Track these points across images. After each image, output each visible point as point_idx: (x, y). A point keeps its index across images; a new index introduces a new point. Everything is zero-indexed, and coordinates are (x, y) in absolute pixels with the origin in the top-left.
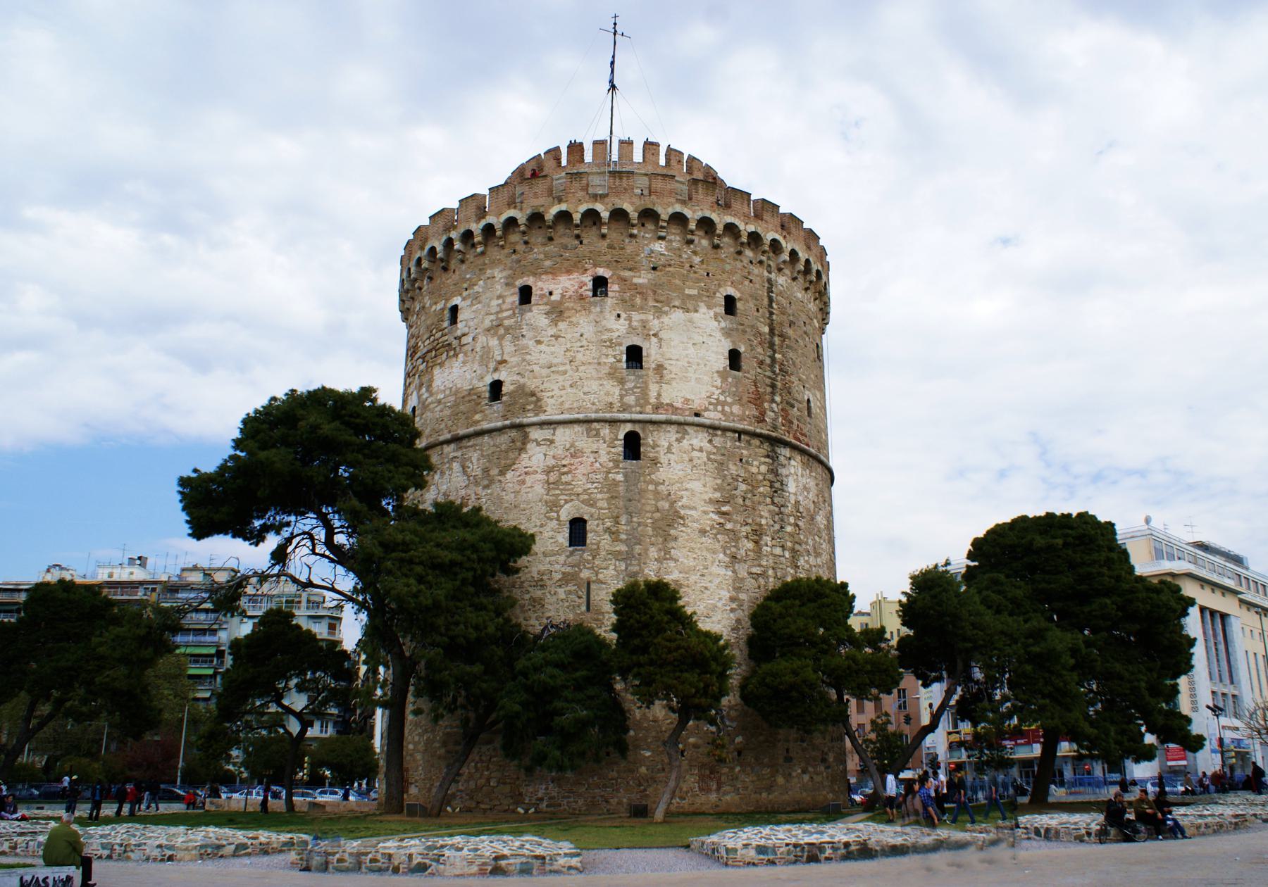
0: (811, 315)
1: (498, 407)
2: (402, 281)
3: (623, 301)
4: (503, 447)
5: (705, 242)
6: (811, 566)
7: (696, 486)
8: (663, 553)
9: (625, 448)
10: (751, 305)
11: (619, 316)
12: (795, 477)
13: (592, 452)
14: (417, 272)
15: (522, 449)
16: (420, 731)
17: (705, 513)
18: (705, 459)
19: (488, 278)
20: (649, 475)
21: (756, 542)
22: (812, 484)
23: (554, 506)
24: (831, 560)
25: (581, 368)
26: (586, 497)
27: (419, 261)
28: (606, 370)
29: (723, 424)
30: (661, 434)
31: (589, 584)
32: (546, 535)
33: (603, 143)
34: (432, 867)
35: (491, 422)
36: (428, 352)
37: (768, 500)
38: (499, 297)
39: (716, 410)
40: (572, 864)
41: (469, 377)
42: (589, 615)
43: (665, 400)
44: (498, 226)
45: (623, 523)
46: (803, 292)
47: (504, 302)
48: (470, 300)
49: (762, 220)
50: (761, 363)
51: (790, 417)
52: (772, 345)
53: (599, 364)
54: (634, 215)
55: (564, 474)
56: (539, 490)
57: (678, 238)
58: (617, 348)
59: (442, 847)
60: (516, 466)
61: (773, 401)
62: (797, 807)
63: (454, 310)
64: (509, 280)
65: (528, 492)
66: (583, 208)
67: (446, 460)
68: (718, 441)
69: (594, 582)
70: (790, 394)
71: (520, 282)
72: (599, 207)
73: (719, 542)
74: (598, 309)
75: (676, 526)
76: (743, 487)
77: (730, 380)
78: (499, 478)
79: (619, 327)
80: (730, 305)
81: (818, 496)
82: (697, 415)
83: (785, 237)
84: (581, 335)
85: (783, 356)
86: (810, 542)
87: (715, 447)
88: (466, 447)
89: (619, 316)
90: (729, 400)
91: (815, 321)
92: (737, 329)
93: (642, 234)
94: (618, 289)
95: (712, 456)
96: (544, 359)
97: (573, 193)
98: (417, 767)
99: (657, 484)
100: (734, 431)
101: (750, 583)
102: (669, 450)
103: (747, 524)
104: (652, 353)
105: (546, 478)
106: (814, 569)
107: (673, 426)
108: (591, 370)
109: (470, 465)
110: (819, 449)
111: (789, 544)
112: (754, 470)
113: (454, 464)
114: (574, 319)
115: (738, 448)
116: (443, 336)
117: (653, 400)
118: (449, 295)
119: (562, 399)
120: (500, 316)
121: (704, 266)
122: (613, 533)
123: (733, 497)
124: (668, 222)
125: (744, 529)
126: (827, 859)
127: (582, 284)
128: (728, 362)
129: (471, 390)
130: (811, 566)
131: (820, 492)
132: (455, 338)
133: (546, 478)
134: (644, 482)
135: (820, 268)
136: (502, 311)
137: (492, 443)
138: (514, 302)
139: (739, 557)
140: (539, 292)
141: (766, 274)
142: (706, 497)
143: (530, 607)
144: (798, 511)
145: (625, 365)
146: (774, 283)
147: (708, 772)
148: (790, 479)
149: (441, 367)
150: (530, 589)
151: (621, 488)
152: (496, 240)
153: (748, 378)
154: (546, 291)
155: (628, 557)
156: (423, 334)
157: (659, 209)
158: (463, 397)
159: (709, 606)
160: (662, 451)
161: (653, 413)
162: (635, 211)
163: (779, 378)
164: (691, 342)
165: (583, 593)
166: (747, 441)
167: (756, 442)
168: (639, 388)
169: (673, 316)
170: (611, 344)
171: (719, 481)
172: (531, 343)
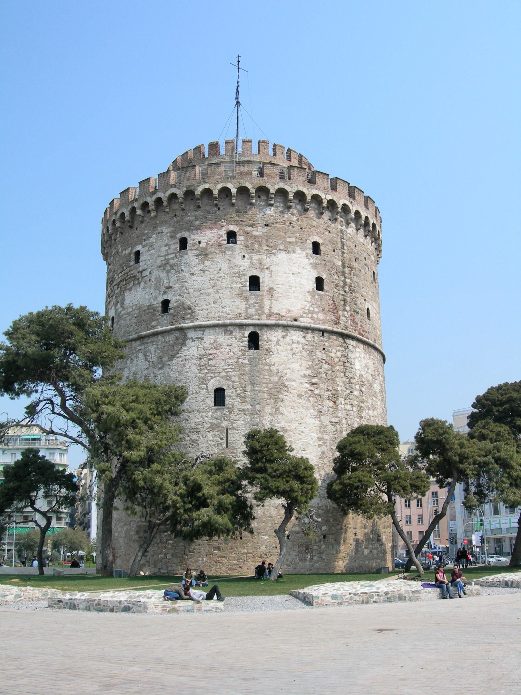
0: (370, 253)
1: (166, 317)
2: (103, 235)
3: (247, 246)
4: (171, 343)
5: (299, 207)
6: (370, 417)
7: (295, 366)
8: (274, 410)
9: (250, 341)
10: (330, 248)
11: (244, 256)
12: (360, 359)
13: (228, 345)
14: (113, 229)
15: (183, 344)
16: (122, 524)
17: (301, 383)
18: (301, 349)
19: (159, 233)
20: (265, 359)
21: (335, 402)
22: (370, 363)
23: (204, 381)
24: (383, 412)
25: (220, 291)
26: (225, 374)
27: (114, 222)
28: (236, 292)
29: (313, 326)
30: (272, 333)
31: (227, 430)
32: (199, 399)
33: (232, 142)
34: (134, 609)
35: (163, 327)
36: (121, 281)
37: (342, 374)
38: (166, 245)
39: (307, 317)
40: (218, 607)
41: (148, 297)
42: (227, 450)
43: (276, 311)
44: (165, 199)
45: (249, 391)
46: (364, 238)
47: (169, 249)
48: (148, 247)
49: (336, 191)
50: (337, 285)
51: (356, 320)
52: (343, 273)
53: (232, 288)
54: (252, 191)
55: (210, 360)
56: (194, 369)
57: (282, 205)
58: (243, 277)
59: (139, 596)
60: (179, 355)
61: (345, 310)
62: (361, 570)
63: (138, 254)
64: (173, 234)
65: (188, 372)
66: (220, 186)
67: (134, 351)
68: (309, 336)
69: (230, 429)
70: (356, 305)
71: (179, 236)
72: (230, 186)
73: (310, 402)
74: (230, 252)
75: (282, 392)
76: (326, 366)
77: (317, 297)
78: (170, 363)
79: (244, 264)
80: (316, 248)
81: (374, 371)
82: (296, 320)
83: (351, 202)
84: (220, 270)
85: (351, 280)
86: (370, 401)
87: (307, 341)
88: (147, 344)
89: (244, 256)
90: (316, 310)
91: (372, 256)
92: (321, 264)
93: (258, 202)
94: (243, 239)
95: (306, 347)
96: (197, 285)
97: (213, 176)
98: (121, 547)
99: (270, 365)
100: (320, 330)
101: (331, 428)
102: (278, 344)
103: (328, 390)
104: (265, 282)
105: (199, 362)
106: (372, 418)
107: (280, 328)
108: (227, 292)
109: (150, 355)
110: (375, 340)
111: (356, 403)
112: (333, 355)
113: (140, 354)
114: (214, 259)
115: (322, 341)
116: (130, 271)
117: (267, 311)
118: (134, 244)
119: (209, 311)
120: (167, 258)
121: (299, 223)
122: (242, 397)
123: (320, 373)
124: (275, 194)
125: (327, 393)
126: (374, 602)
127: (220, 236)
128: (315, 285)
129: (149, 306)
130: (370, 417)
131: (376, 369)
132: (138, 272)
133: (199, 362)
134: (262, 364)
135: (375, 222)
136: (168, 254)
137: (163, 340)
138: (176, 248)
139: (323, 411)
140: (192, 242)
141: (339, 227)
142: (302, 373)
143: (190, 446)
145: (248, 288)
146: (344, 232)
147: (304, 549)
148: (356, 360)
149: (130, 291)
150: (189, 434)
151: (246, 369)
152: (163, 208)
153: (328, 296)
154: (196, 241)
155: (253, 413)
156: (117, 270)
157: (269, 186)
158: (144, 311)
159: (305, 443)
160: (273, 344)
161: (267, 319)
162: (253, 188)
163: (349, 295)
164: (291, 273)
165: (224, 436)
167: (335, 337)
168: (257, 303)
169: (279, 256)
170: (239, 275)
171: (310, 363)
172: (188, 275)
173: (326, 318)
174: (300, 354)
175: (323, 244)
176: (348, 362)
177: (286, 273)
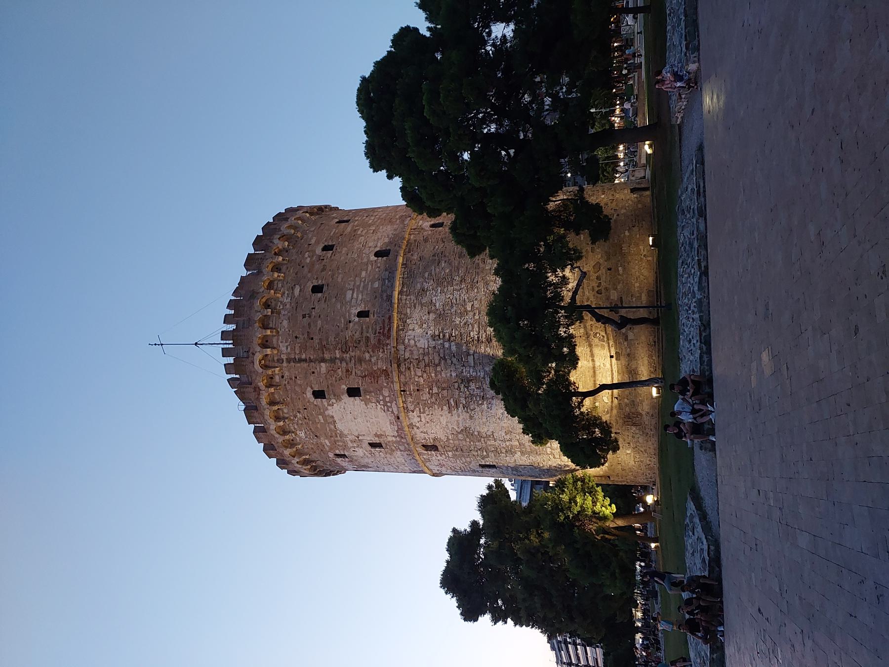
7: (444, 420)
10: (312, 378)
17: (459, 416)
37: (439, 369)
39: (391, 407)
52: (333, 360)
68: (411, 407)
70: (360, 341)
76: (435, 390)
77: (368, 397)
80: (319, 394)
83: (253, 354)
95: (422, 410)
103: (459, 388)
112: (421, 380)
139: (482, 394)
141: (285, 364)
144: (440, 338)
164: (353, 419)
166: (404, 385)
173: (386, 387)
174: (430, 416)
175: (311, 386)
176: (423, 359)
177: (356, 424)
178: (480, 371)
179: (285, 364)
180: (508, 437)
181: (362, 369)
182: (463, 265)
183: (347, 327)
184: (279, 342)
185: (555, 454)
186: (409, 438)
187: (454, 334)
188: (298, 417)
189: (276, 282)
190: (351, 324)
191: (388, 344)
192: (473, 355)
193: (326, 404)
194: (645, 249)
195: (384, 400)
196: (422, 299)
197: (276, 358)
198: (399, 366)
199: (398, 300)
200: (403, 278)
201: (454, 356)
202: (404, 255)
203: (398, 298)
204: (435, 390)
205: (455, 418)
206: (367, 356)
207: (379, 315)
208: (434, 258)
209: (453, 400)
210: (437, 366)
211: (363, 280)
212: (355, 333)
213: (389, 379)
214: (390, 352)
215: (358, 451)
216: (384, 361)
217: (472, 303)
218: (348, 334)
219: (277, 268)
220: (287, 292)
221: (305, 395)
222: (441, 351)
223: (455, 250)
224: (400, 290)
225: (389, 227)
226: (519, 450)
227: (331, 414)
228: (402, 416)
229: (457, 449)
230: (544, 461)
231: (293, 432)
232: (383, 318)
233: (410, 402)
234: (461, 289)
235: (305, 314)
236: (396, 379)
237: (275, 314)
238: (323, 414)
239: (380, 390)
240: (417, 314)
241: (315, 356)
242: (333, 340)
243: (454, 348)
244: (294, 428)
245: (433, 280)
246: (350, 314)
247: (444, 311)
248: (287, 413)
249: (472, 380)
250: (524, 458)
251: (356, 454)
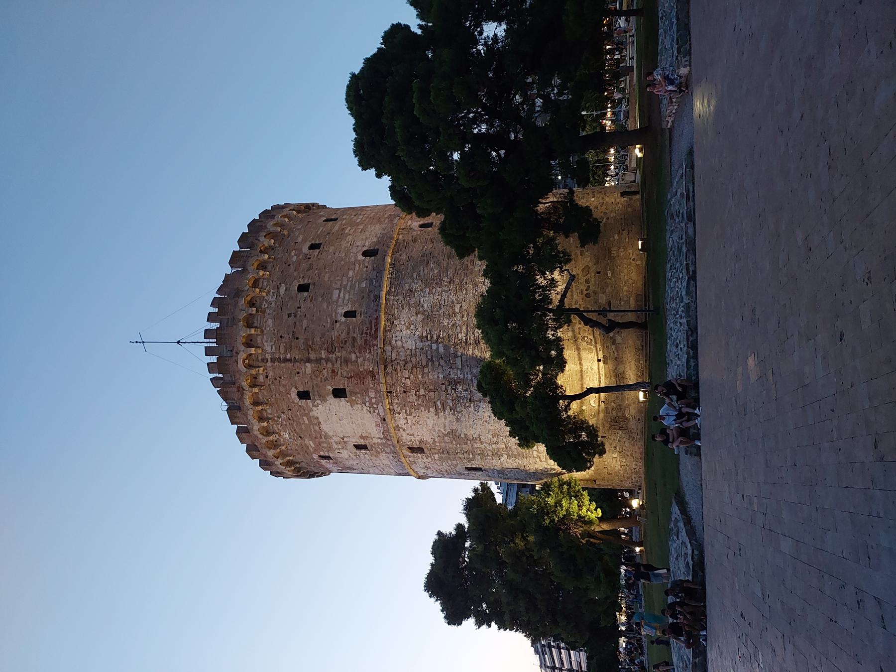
7: (430, 422)
10: (297, 378)
17: (445, 418)
21: (456, 383)
37: (426, 370)
39: (377, 408)
46: (267, 317)
52: (318, 361)
68: (397, 409)
70: (346, 341)
76: (422, 392)
77: (354, 398)
80: (304, 395)
83: (237, 353)
95: (408, 413)
102: (412, 435)
103: (446, 390)
112: (408, 381)
134: (435, 446)
139: (469, 396)
141: (269, 364)
144: (427, 339)
153: (348, 384)
166: (390, 387)
173: (372, 388)
177: (341, 426)
178: (467, 373)
179: (269, 364)
180: (495, 440)
181: (348, 370)
182: (452, 266)
183: (333, 327)
184: (264, 341)
185: (541, 457)
186: (395, 440)
187: (441, 336)
188: (283, 417)
189: (261, 281)
190: (338, 324)
191: (375, 345)
192: (461, 357)
193: (311, 405)
194: (634, 254)
195: (370, 402)
196: (410, 299)
197: (260, 358)
198: (385, 367)
199: (386, 300)
200: (391, 278)
201: (442, 358)
202: (392, 254)
203: (386, 298)
204: (422, 392)
205: (442, 420)
206: (353, 357)
207: (366, 315)
208: (423, 258)
209: (440, 402)
210: (424, 367)
211: (350, 279)
212: (342, 333)
213: (376, 380)
214: (377, 353)
215: (343, 453)
216: (371, 362)
217: (461, 304)
218: (334, 334)
219: (262, 266)
220: (272, 291)
221: (289, 396)
222: (429, 352)
223: (444, 252)
224: (388, 290)
225: (377, 226)
226: (506, 453)
227: (316, 415)
228: (388, 417)
229: (443, 451)
230: (530, 464)
231: (277, 433)
232: (370, 319)
233: (397, 404)
234: (449, 290)
235: (291, 314)
236: (382, 380)
237: (260, 313)
238: (307, 415)
239: (367, 391)
240: (405, 315)
241: (300, 356)
242: (319, 340)
243: (441, 350)
244: (278, 429)
245: (422, 281)
246: (336, 314)
247: (432, 312)
248: (271, 414)
249: (459, 382)
250: (510, 461)
251: (341, 456)
